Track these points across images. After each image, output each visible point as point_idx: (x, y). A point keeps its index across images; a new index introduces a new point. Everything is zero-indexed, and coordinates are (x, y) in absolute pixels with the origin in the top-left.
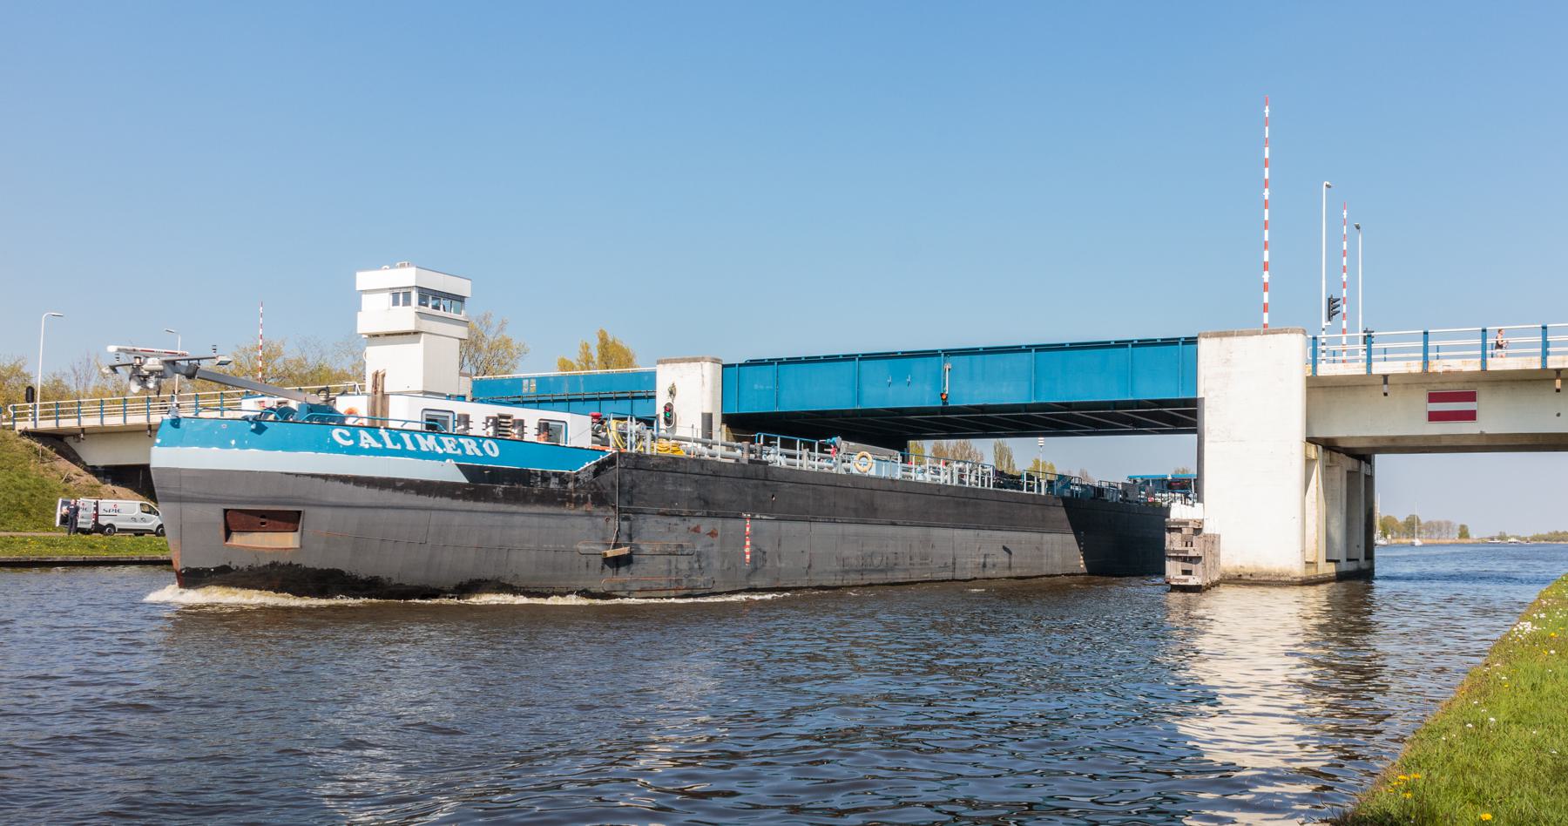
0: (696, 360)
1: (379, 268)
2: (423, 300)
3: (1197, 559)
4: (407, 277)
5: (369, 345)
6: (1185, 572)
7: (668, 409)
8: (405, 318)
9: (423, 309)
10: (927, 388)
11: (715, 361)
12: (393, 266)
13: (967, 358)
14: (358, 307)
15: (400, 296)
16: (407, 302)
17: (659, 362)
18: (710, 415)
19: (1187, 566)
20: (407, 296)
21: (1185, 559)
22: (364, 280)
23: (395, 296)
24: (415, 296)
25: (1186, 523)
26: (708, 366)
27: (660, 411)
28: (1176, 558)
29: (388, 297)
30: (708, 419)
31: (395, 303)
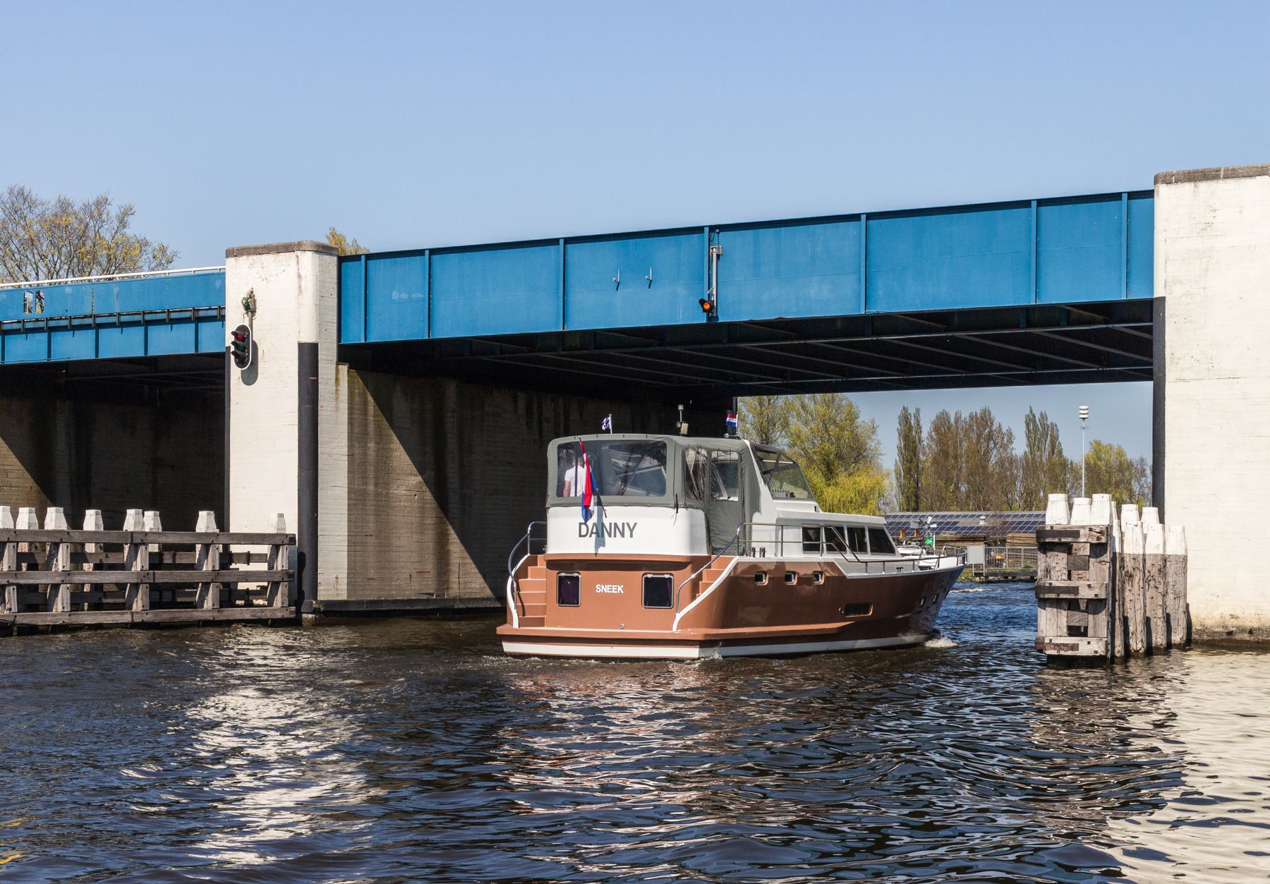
0: (288, 248)
3: (1095, 605)
6: (1074, 631)
7: (242, 336)
10: (682, 291)
11: (322, 250)
13: (750, 232)
17: (231, 253)
18: (313, 348)
19: (1077, 619)
21: (1073, 605)
25: (1075, 534)
26: (308, 260)
27: (229, 339)
28: (1057, 603)
30: (309, 354)
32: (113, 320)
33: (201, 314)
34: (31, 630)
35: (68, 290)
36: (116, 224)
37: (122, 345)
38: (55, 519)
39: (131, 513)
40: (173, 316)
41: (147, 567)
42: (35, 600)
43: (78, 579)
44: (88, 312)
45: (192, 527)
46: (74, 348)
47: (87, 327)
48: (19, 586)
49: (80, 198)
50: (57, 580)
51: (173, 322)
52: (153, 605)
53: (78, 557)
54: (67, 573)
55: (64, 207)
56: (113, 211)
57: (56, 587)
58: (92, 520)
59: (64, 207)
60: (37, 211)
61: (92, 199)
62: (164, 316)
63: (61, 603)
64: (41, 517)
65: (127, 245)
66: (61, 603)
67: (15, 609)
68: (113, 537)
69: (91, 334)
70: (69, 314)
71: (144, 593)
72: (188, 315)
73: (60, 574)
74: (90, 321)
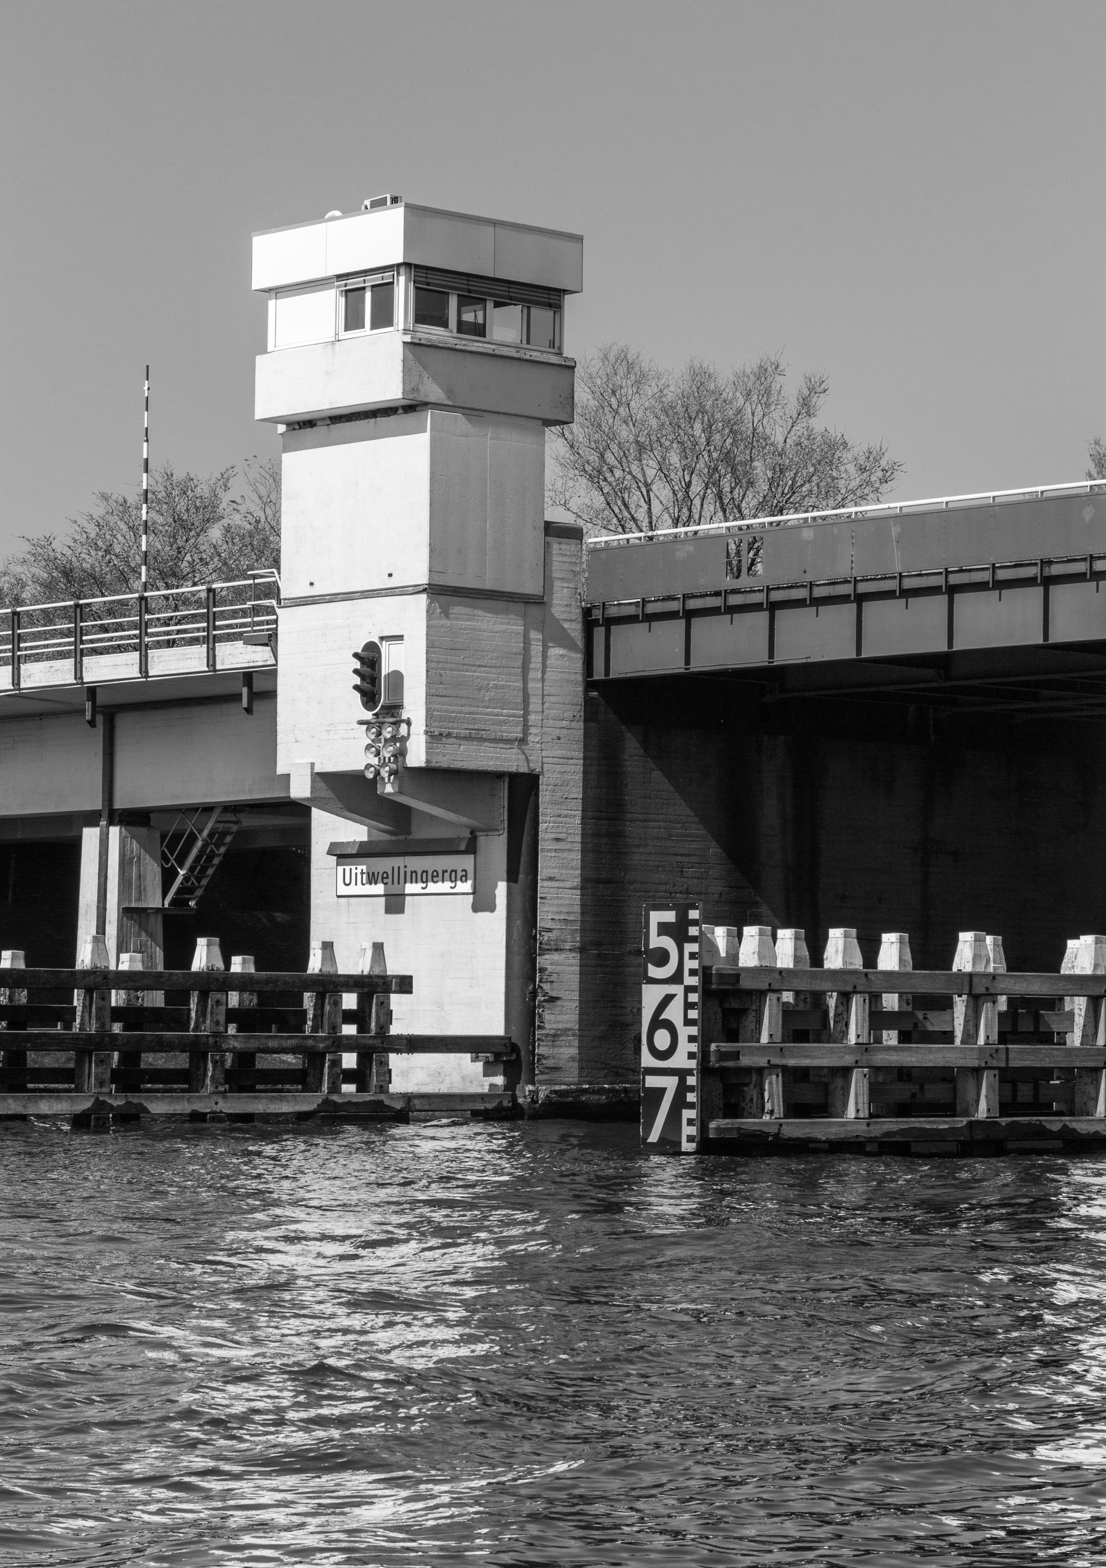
1: (316, 216)
2: (428, 310)
4: (376, 238)
5: (287, 449)
8: (376, 364)
9: (433, 333)
12: (350, 209)
14: (256, 341)
15: (362, 297)
16: (383, 317)
20: (383, 292)
22: (277, 255)
23: (353, 296)
24: (402, 292)
29: (331, 301)
31: (353, 321)
32: (892, 585)
33: (1056, 570)
34: (801, 1148)
35: (808, 534)
36: (793, 407)
37: (905, 631)
38: (839, 948)
39: (966, 938)
40: (1002, 575)
41: (995, 1037)
42: (808, 1095)
43: (881, 1059)
44: (843, 570)
45: (1054, 964)
46: (817, 639)
47: (843, 599)
48: (785, 1069)
49: (728, 365)
50: (848, 1060)
51: (1001, 585)
52: (1005, 1108)
53: (878, 1020)
54: (863, 1048)
55: (700, 378)
56: (790, 387)
57: (845, 1072)
58: (891, 952)
59: (700, 378)
60: (650, 390)
61: (751, 365)
62: (986, 576)
63: (855, 1105)
64: (816, 947)
65: (830, 452)
66: (855, 1105)
67: (779, 1111)
68: (929, 982)
69: (848, 611)
70: (808, 578)
71: (989, 1087)
72: (1031, 572)
73: (850, 1050)
74: (846, 589)
